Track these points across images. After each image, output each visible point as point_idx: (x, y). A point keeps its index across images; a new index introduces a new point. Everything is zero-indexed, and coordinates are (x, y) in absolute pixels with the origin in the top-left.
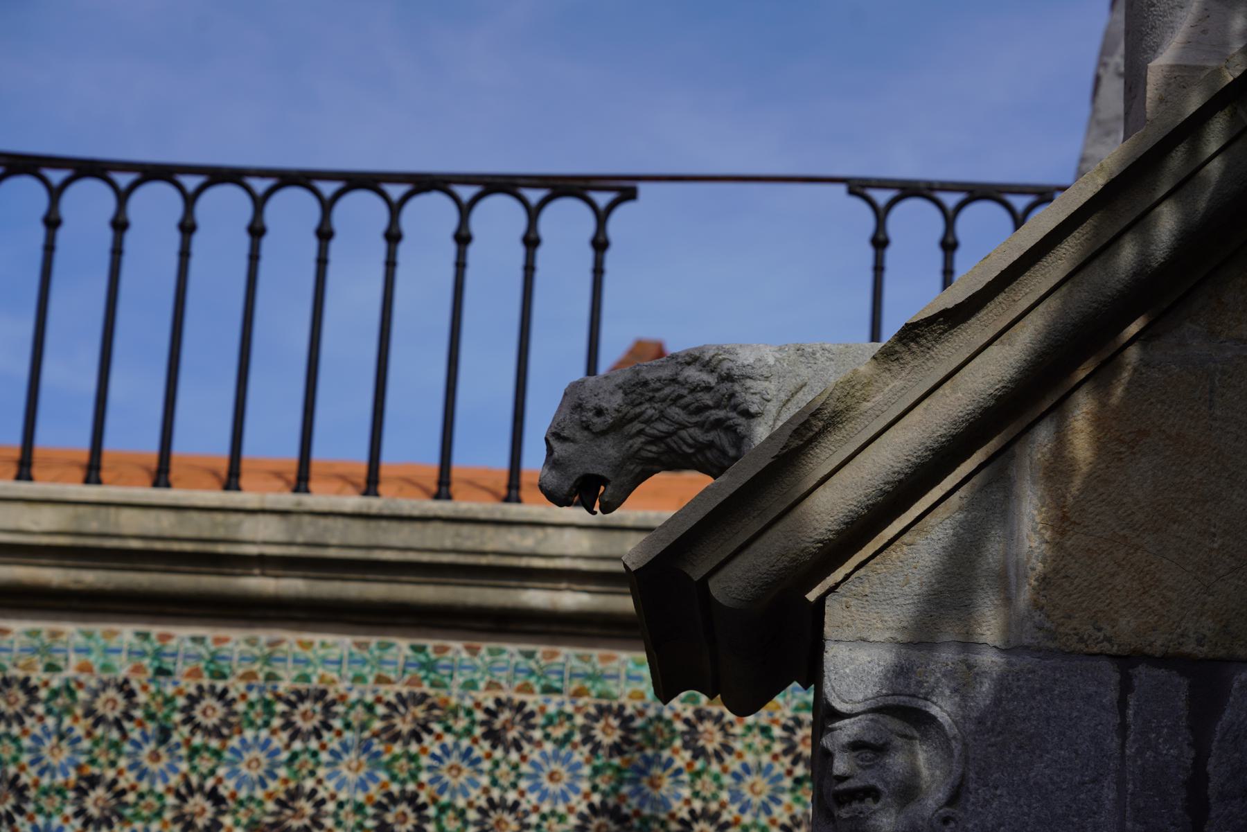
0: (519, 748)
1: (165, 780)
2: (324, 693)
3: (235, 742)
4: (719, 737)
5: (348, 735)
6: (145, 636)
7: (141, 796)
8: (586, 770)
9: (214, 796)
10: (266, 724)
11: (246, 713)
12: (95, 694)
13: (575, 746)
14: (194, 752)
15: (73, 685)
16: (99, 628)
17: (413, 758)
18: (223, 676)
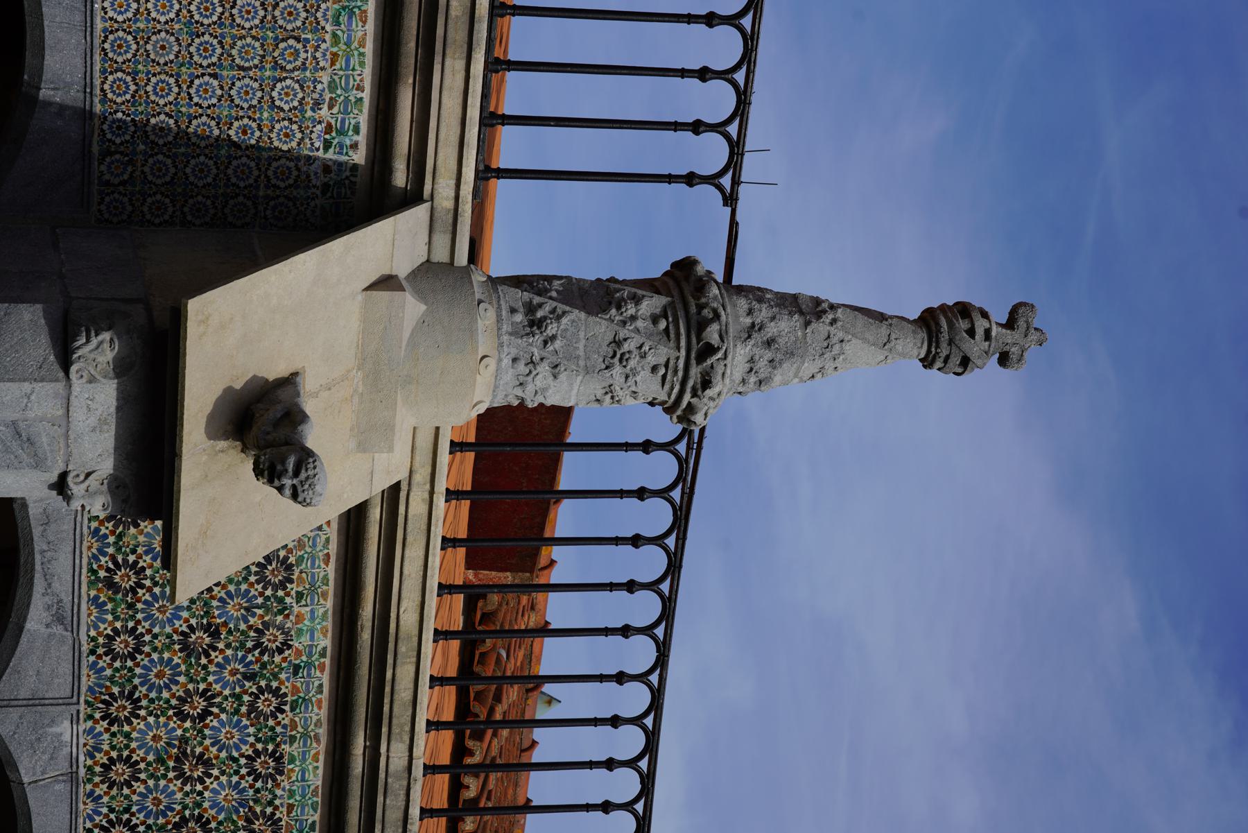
1: (216, 682)
2: (281, 773)
3: (245, 722)
5: (251, 792)
6: (323, 655)
7: (205, 667)
9: (206, 713)
10: (258, 740)
11: (266, 726)
12: (280, 628)
14: (238, 697)
16: (329, 624)
18: (292, 709)
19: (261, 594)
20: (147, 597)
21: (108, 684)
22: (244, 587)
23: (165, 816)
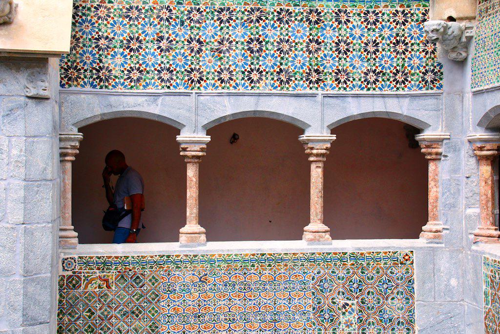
0: (288, 23)
1: (184, 37)
2: (229, 9)
3: (204, 25)
4: (346, 18)
5: (237, 21)
8: (308, 29)
9: (199, 41)
13: (304, 22)
14: (192, 28)
15: (152, 8)
17: (257, 28)
18: (198, 4)
19: (144, 19)
20: (144, 66)
21: (183, 81)
22: (140, 26)
23: (247, 57)
